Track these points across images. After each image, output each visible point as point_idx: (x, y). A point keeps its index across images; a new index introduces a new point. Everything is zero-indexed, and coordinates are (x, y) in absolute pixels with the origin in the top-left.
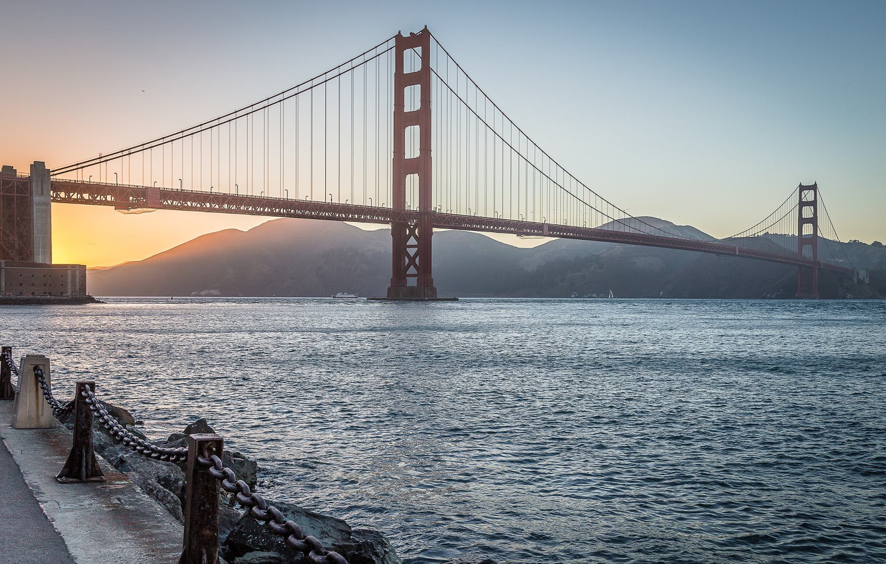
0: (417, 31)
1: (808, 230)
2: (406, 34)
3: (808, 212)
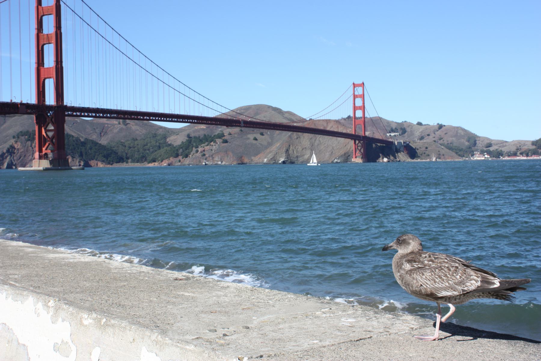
1: (359, 114)
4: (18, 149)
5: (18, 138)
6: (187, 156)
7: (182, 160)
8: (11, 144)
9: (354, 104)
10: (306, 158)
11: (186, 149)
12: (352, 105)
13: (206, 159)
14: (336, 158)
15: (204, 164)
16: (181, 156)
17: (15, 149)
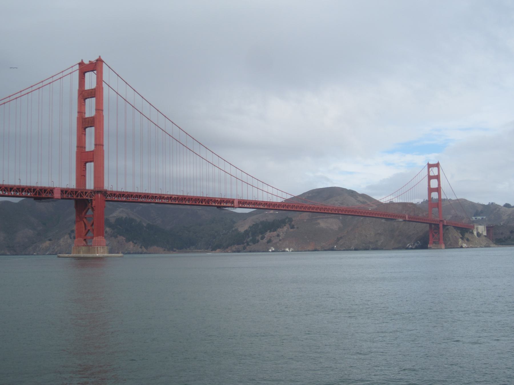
0: (94, 59)
1: (435, 195)
2: (86, 62)
3: (434, 184)
9: (429, 185)
12: (427, 187)
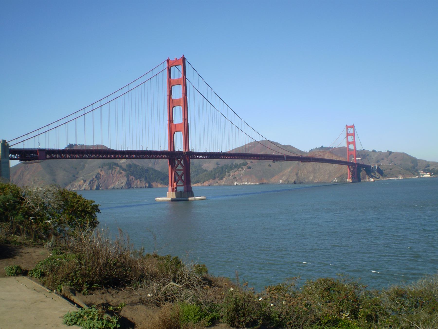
1: (351, 147)
3: (351, 139)
4: (103, 176)
5: (102, 167)
6: (222, 179)
7: (219, 182)
8: (98, 172)
9: (347, 140)
10: (311, 179)
11: (221, 174)
13: (236, 181)
14: (334, 179)
15: (235, 184)
16: (218, 179)
17: (100, 175)
